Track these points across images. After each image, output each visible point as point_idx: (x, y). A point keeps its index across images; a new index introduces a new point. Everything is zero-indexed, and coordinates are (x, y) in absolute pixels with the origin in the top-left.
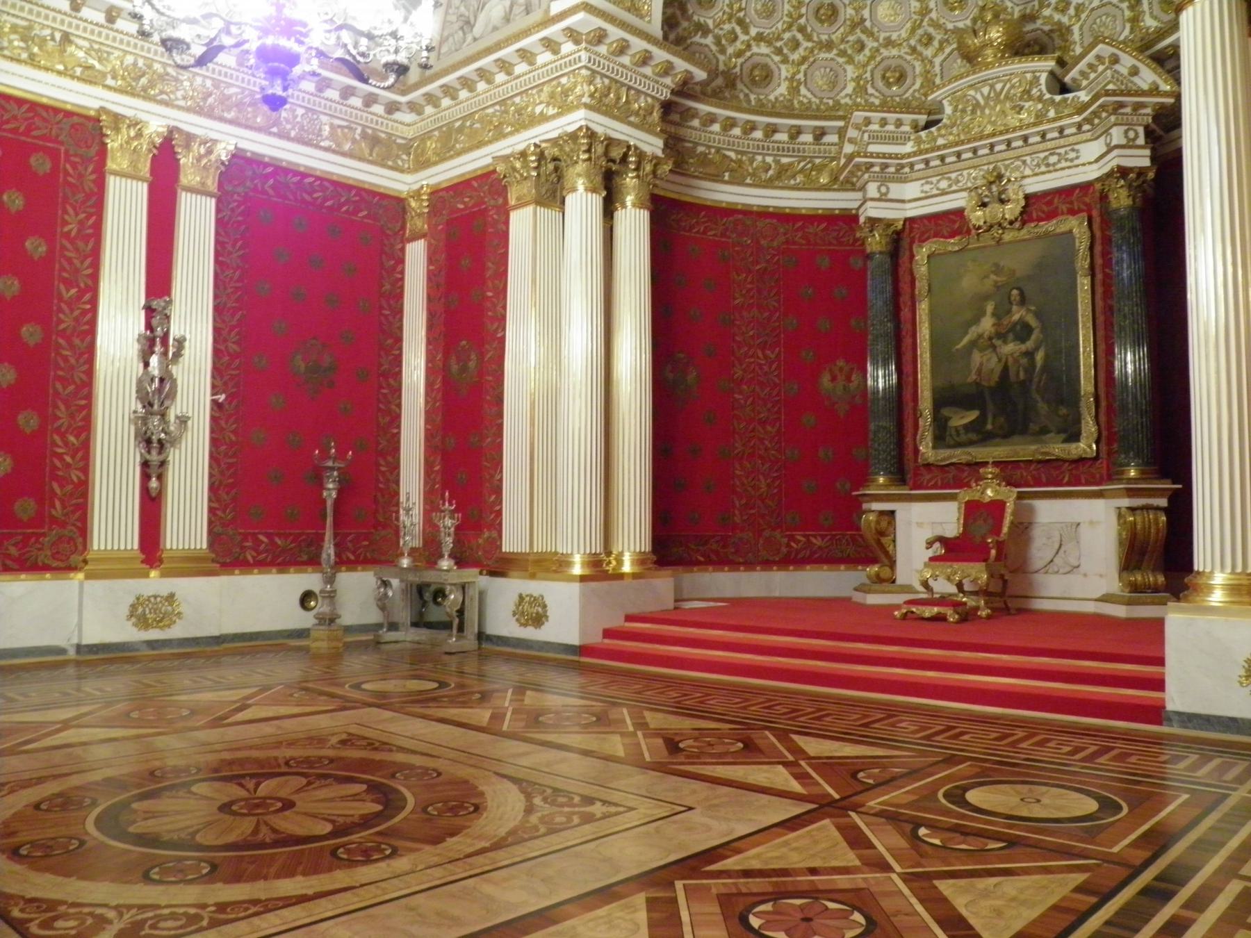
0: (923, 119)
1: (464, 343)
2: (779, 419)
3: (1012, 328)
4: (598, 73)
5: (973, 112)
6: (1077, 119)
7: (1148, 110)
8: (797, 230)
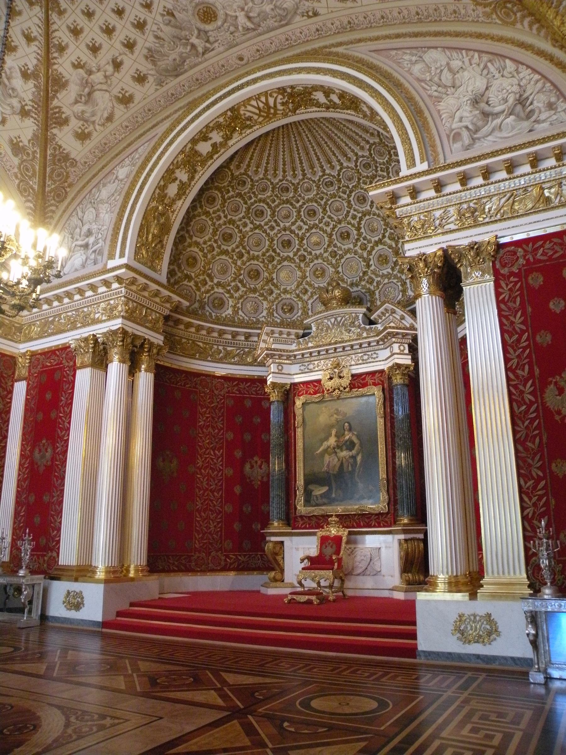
0: (301, 332)
1: (44, 441)
2: (221, 489)
3: (344, 444)
4: (131, 300)
5: (327, 331)
6: (377, 338)
7: (410, 337)
8: (234, 386)
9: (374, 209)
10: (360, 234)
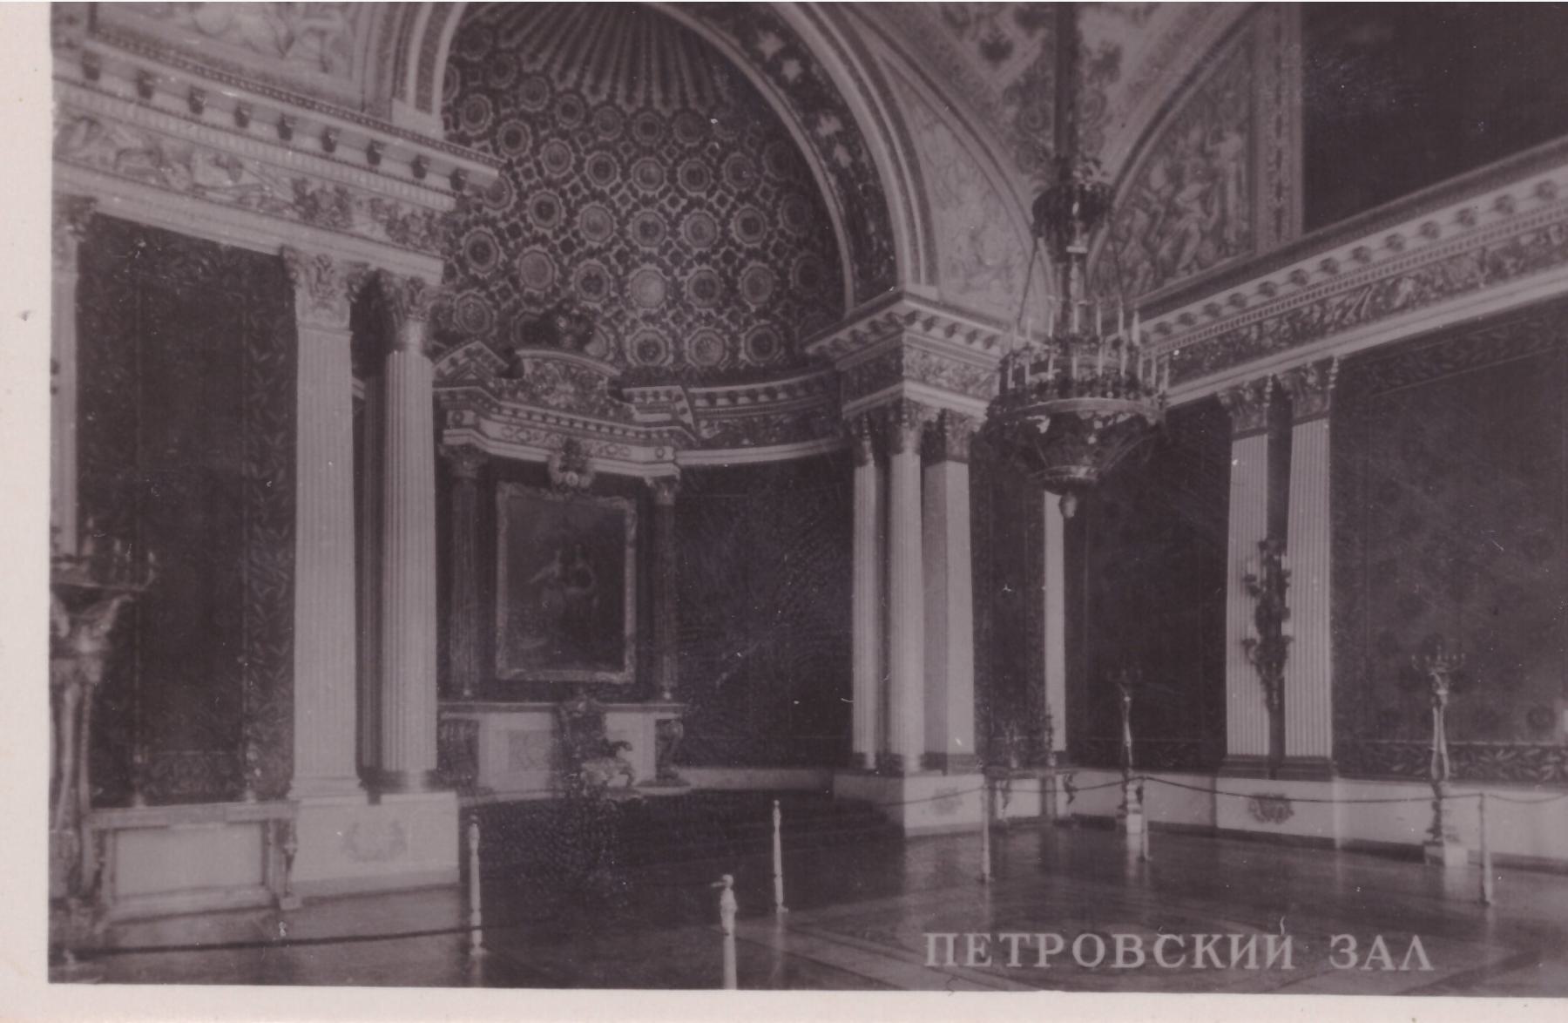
9: (615, 198)
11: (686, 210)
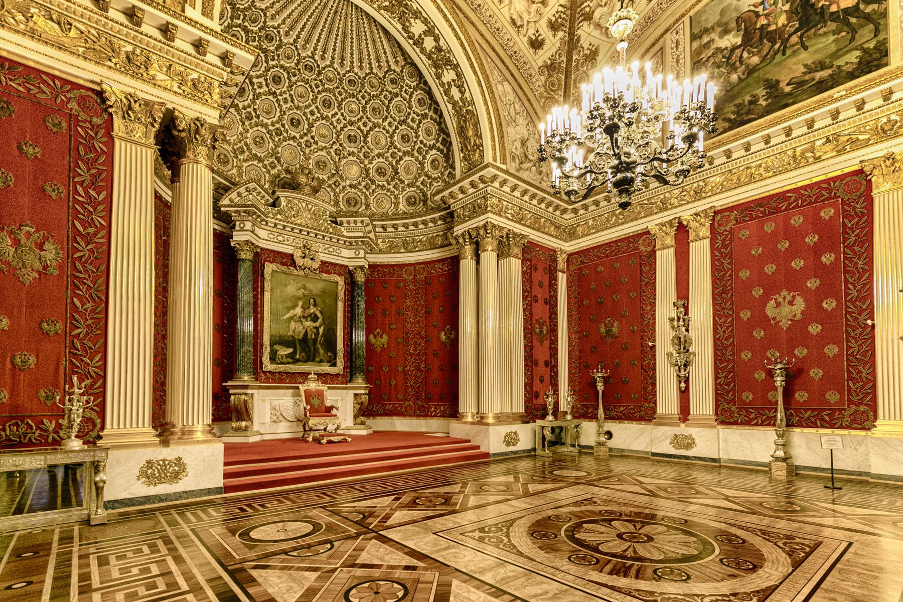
3: (310, 316)
9: (334, 120)
10: (309, 131)
11: (371, 129)
